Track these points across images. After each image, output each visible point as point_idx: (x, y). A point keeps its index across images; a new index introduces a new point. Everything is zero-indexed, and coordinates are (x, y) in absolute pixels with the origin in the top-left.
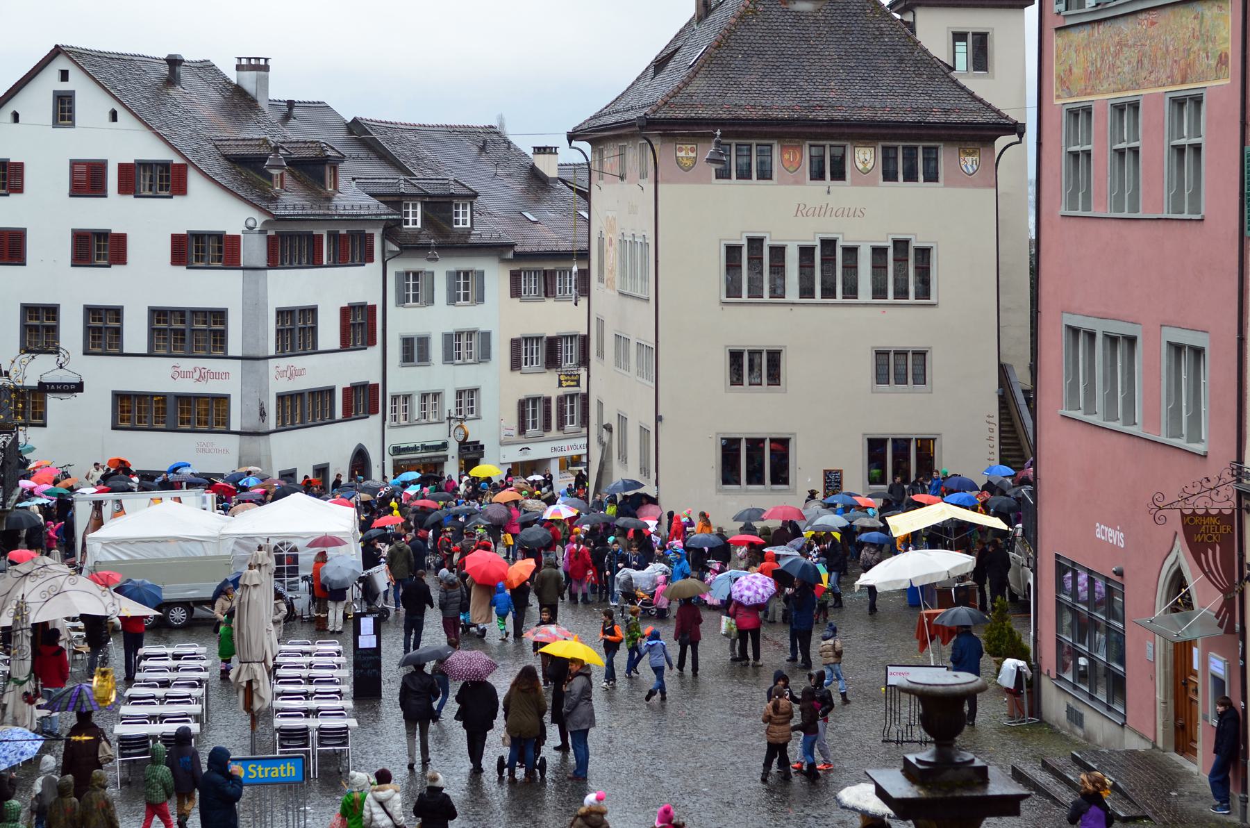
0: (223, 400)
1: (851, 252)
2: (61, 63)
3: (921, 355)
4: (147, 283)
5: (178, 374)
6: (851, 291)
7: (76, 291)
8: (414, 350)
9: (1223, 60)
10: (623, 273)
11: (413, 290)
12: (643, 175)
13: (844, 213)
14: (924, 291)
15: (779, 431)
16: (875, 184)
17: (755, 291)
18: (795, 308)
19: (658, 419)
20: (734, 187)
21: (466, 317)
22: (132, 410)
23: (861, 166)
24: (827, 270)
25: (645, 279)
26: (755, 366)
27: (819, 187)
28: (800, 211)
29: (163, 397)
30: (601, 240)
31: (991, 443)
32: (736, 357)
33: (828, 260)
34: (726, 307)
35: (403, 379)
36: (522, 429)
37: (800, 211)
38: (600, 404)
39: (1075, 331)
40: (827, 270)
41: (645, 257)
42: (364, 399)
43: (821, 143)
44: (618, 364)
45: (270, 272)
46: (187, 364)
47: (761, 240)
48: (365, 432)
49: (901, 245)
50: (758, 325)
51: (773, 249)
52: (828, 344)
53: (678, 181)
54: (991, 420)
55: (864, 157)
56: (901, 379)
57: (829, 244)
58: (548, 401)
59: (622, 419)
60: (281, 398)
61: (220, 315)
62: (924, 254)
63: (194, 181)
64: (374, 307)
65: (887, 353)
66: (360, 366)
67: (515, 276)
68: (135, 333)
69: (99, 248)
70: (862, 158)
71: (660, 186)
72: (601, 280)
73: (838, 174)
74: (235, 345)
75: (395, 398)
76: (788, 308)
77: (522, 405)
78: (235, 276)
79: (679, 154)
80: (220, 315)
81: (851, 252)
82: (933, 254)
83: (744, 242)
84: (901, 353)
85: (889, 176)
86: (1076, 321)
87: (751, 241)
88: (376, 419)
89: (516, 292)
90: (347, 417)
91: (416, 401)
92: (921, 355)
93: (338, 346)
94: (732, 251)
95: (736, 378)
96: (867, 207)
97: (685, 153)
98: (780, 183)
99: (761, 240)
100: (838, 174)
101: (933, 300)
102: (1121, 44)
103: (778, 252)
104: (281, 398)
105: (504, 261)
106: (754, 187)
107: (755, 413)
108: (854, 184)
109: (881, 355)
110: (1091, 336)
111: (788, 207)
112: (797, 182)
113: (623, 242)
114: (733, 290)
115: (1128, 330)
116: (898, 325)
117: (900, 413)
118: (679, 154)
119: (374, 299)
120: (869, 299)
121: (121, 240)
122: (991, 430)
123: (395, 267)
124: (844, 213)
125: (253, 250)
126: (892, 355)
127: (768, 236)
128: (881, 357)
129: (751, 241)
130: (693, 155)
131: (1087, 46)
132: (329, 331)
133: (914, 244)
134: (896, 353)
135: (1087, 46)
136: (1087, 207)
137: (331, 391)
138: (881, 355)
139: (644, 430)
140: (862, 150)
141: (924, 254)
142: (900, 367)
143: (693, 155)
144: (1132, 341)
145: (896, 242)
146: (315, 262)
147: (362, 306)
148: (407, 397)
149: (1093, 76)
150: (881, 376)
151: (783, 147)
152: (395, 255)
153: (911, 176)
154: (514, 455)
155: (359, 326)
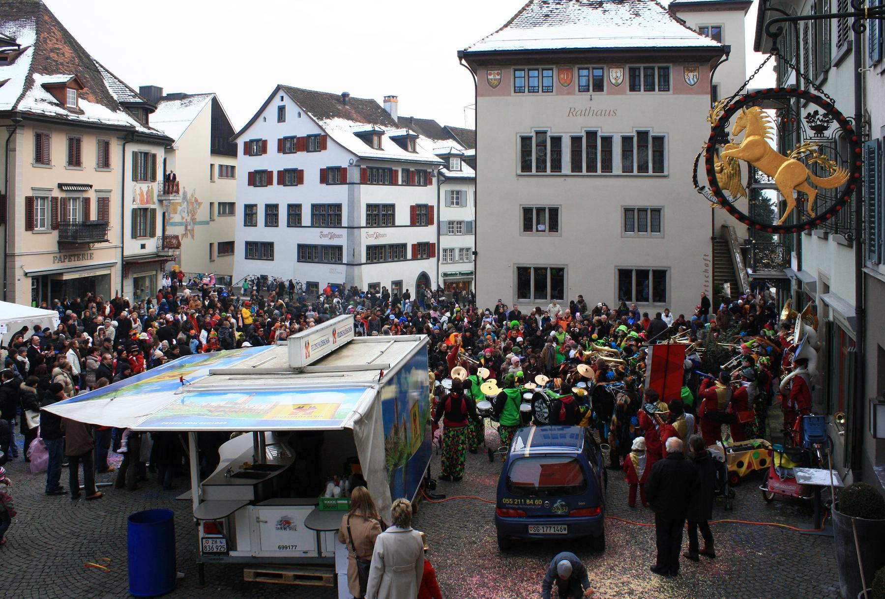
0: (340, 248)
1: (607, 141)
2: (281, 93)
3: (656, 212)
4: (312, 193)
5: (322, 235)
6: (607, 166)
7: (282, 196)
8: (455, 227)
11: (456, 199)
13: (602, 113)
14: (659, 166)
16: (624, 93)
17: (541, 167)
18: (568, 179)
22: (306, 253)
23: (613, 81)
26: (540, 218)
28: (571, 112)
29: (315, 247)
31: (707, 274)
32: (527, 212)
33: (592, 146)
34: (520, 179)
35: (447, 241)
37: (571, 112)
42: (424, 250)
43: (586, 66)
45: (363, 187)
46: (326, 231)
47: (545, 132)
48: (428, 266)
49: (643, 135)
50: (543, 190)
52: (592, 204)
53: (489, 95)
54: (706, 258)
55: (616, 75)
56: (642, 228)
57: (592, 135)
60: (369, 248)
61: (338, 207)
62: (659, 141)
63: (329, 143)
64: (432, 207)
65: (633, 210)
66: (426, 234)
68: (306, 217)
69: (292, 177)
70: (614, 76)
74: (345, 223)
75: (445, 250)
76: (562, 179)
78: (344, 188)
79: (490, 77)
80: (338, 207)
81: (607, 141)
82: (666, 140)
84: (642, 211)
85: (634, 88)
87: (537, 133)
88: (433, 260)
90: (415, 258)
91: (457, 252)
92: (657, 212)
93: (409, 224)
95: (528, 226)
98: (557, 94)
99: (545, 132)
101: (666, 173)
103: (557, 141)
104: (369, 248)
106: (541, 98)
107: (540, 250)
108: (608, 93)
109: (628, 211)
112: (569, 94)
114: (526, 166)
117: (642, 252)
118: (490, 77)
119: (432, 202)
120: (620, 173)
121: (301, 173)
122: (707, 265)
123: (444, 188)
124: (602, 113)
125: (354, 175)
126: (636, 211)
127: (549, 130)
128: (628, 213)
129: (537, 133)
130: (498, 77)
132: (403, 216)
133: (651, 134)
134: (639, 210)
137: (404, 246)
138: (628, 211)
140: (614, 70)
141: (659, 141)
142: (642, 220)
143: (498, 77)
145: (639, 133)
146: (393, 182)
147: (426, 206)
148: (452, 250)
150: (628, 226)
152: (444, 182)
153: (650, 88)
155: (422, 215)
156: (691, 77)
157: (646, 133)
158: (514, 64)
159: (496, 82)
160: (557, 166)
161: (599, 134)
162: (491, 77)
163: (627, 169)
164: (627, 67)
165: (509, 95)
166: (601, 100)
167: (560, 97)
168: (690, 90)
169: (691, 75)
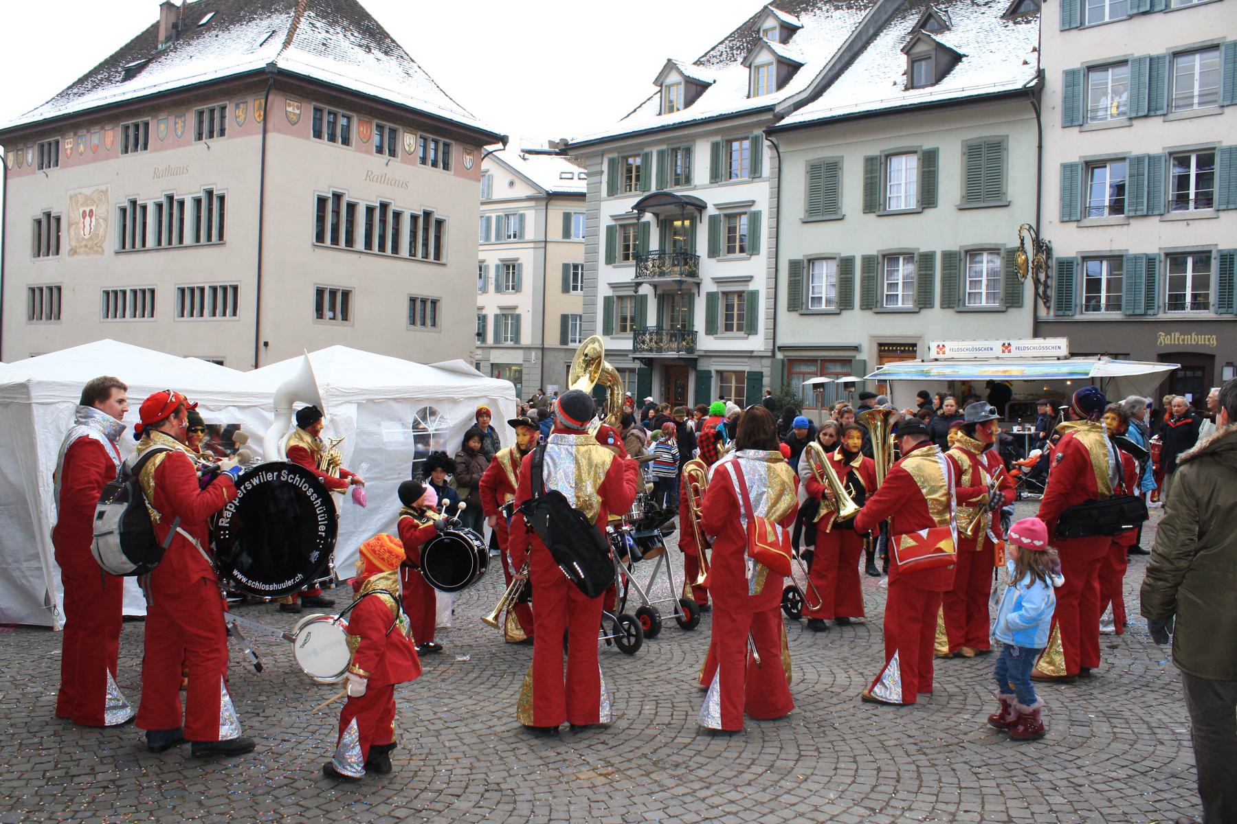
1: (397, 215)
3: (434, 303)
16: (414, 165)
20: (323, 145)
34: (317, 250)
49: (427, 215)
55: (409, 141)
57: (384, 206)
62: (439, 223)
71: (270, 136)
73: (393, 153)
76: (356, 256)
83: (330, 195)
94: (322, 201)
97: (293, 108)
101: (443, 260)
106: (338, 149)
108: (402, 161)
112: (367, 152)
141: (439, 223)
143: (298, 112)
151: (360, 121)
153: (435, 164)
156: (468, 160)
158: (316, 100)
159: (295, 118)
162: (290, 109)
164: (419, 133)
165: (308, 138)
166: (397, 168)
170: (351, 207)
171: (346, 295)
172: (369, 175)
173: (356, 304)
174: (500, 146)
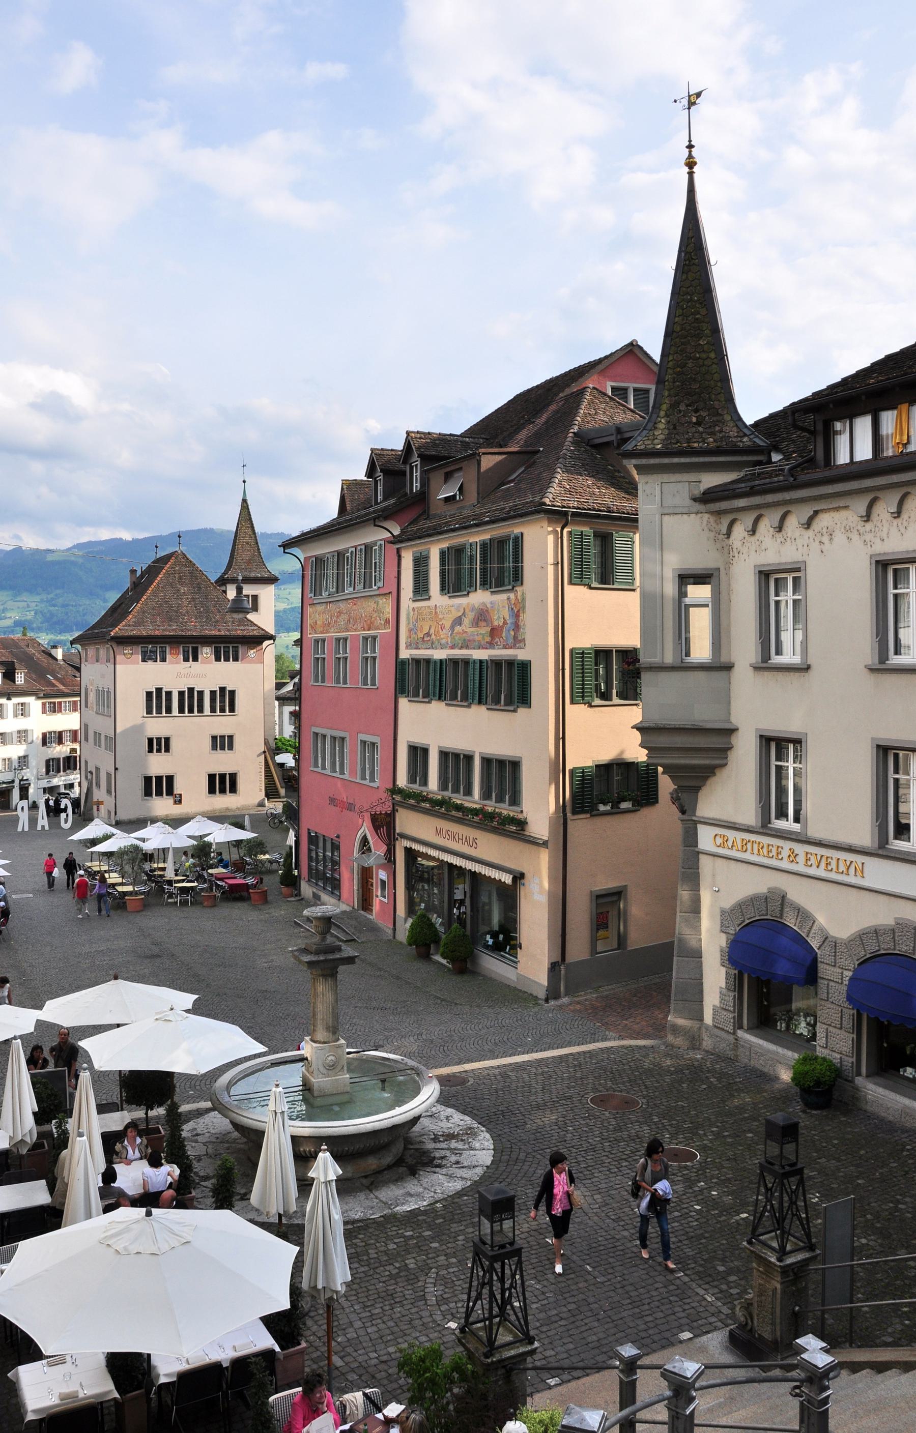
1: (201, 693)
3: (231, 738)
6: (201, 710)
9: (387, 621)
10: (98, 704)
12: (108, 661)
14: (232, 709)
15: (169, 772)
16: (211, 663)
17: (159, 711)
19: (116, 769)
21: (21, 723)
24: (191, 701)
25: (109, 707)
26: (159, 745)
27: (187, 664)
30: (86, 689)
36: (48, 772)
37: (179, 675)
38: (86, 762)
39: (316, 734)
40: (191, 701)
41: (109, 697)
44: (95, 744)
49: (223, 689)
51: (166, 692)
56: (222, 748)
57: (191, 690)
58: (59, 759)
59: (97, 769)
67: (44, 704)
71: (118, 666)
72: (86, 706)
73: (195, 659)
77: (48, 762)
84: (222, 737)
85: (218, 659)
86: (317, 730)
89: (44, 712)
94: (149, 694)
96: (208, 673)
100: (195, 659)
102: (340, 613)
105: (39, 698)
109: (214, 738)
110: (324, 736)
111: (174, 673)
113: (98, 691)
114: (149, 711)
115: (342, 734)
116: (221, 724)
117: (223, 763)
131: (324, 613)
135: (324, 613)
136: (323, 681)
138: (214, 738)
139: (109, 775)
141: (232, 693)
142: (222, 743)
144: (343, 739)
145: (220, 688)
149: (327, 626)
151: (171, 648)
154: (44, 784)
156: (252, 653)
157: (225, 688)
160: (169, 710)
161: (196, 689)
163: (213, 710)
167: (171, 666)
168: (252, 661)
169: (252, 652)
170: (169, 694)
171: (167, 740)
172: (179, 675)
173: (173, 744)
174: (272, 641)
